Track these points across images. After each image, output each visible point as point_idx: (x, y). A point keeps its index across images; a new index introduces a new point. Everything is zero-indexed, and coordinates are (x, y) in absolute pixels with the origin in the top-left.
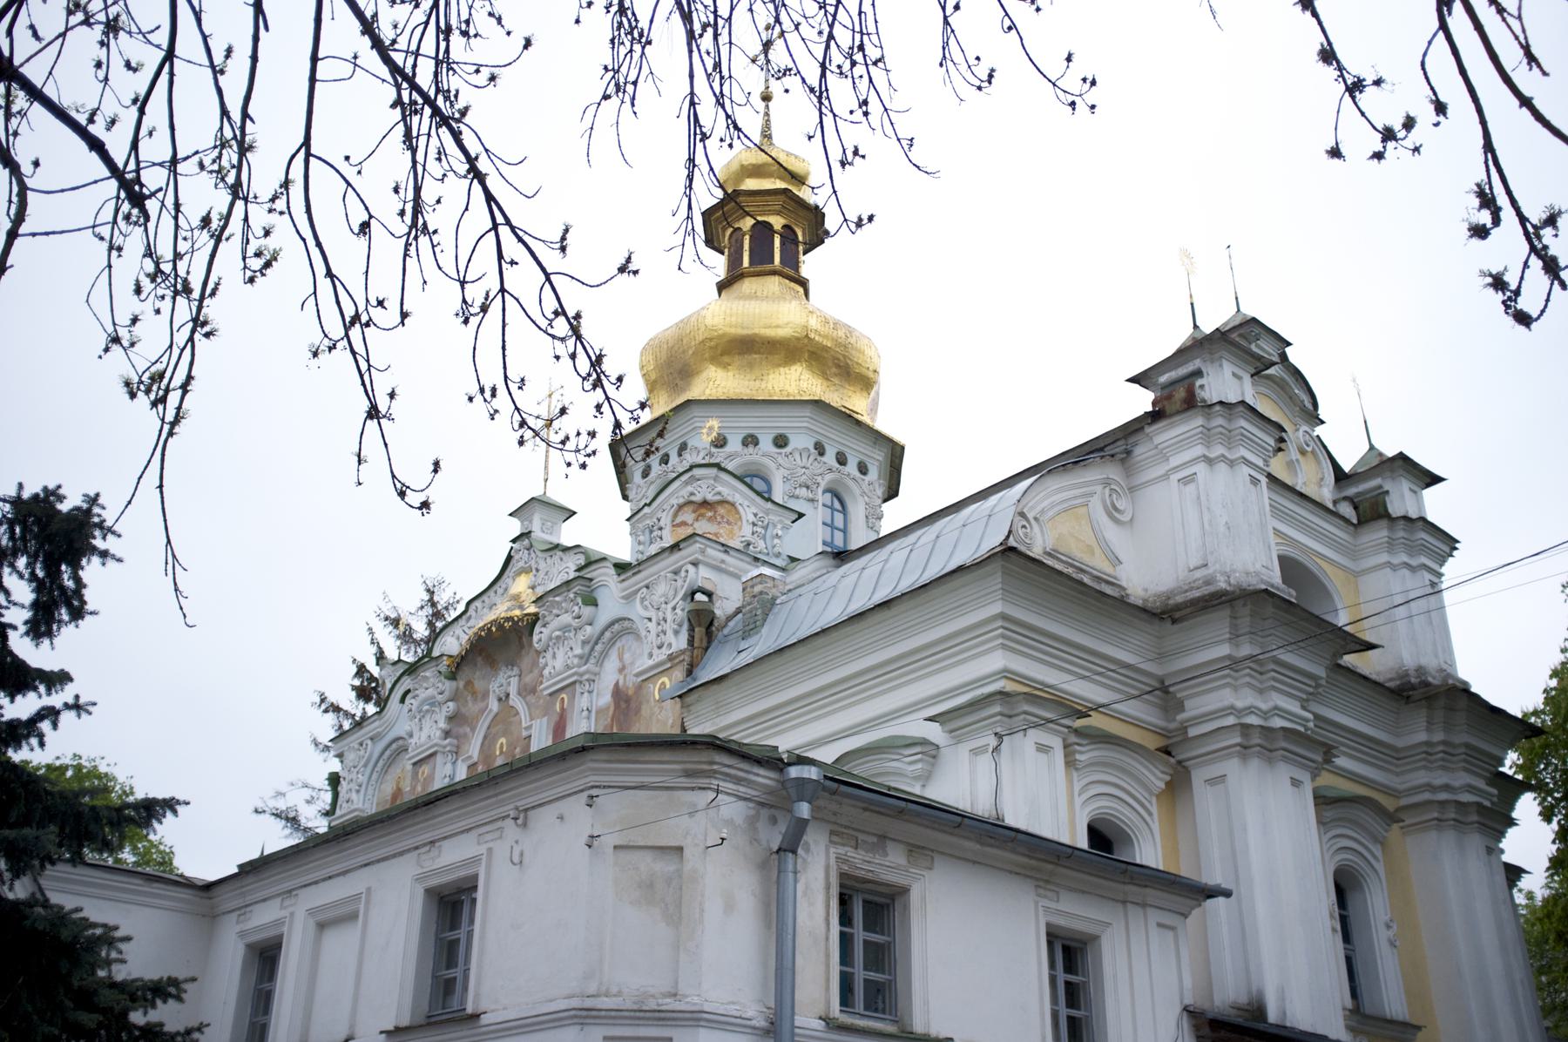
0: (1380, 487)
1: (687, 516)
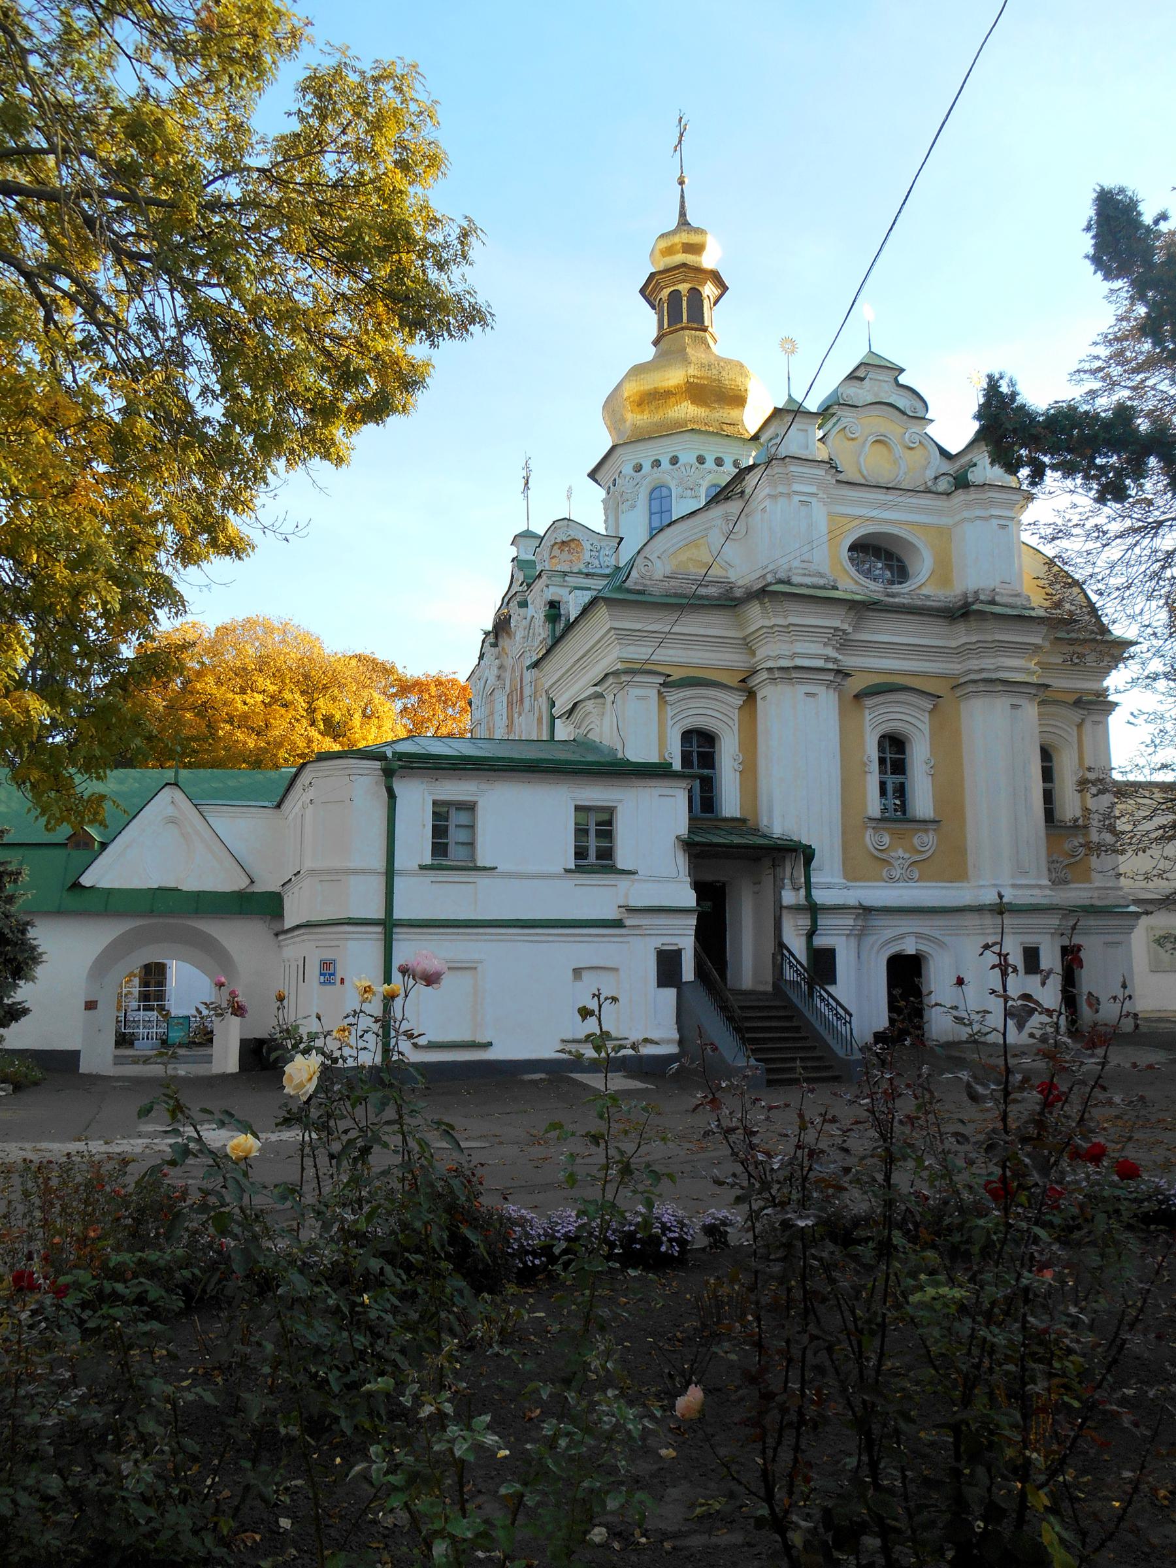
0: (971, 460)
1: (556, 552)
